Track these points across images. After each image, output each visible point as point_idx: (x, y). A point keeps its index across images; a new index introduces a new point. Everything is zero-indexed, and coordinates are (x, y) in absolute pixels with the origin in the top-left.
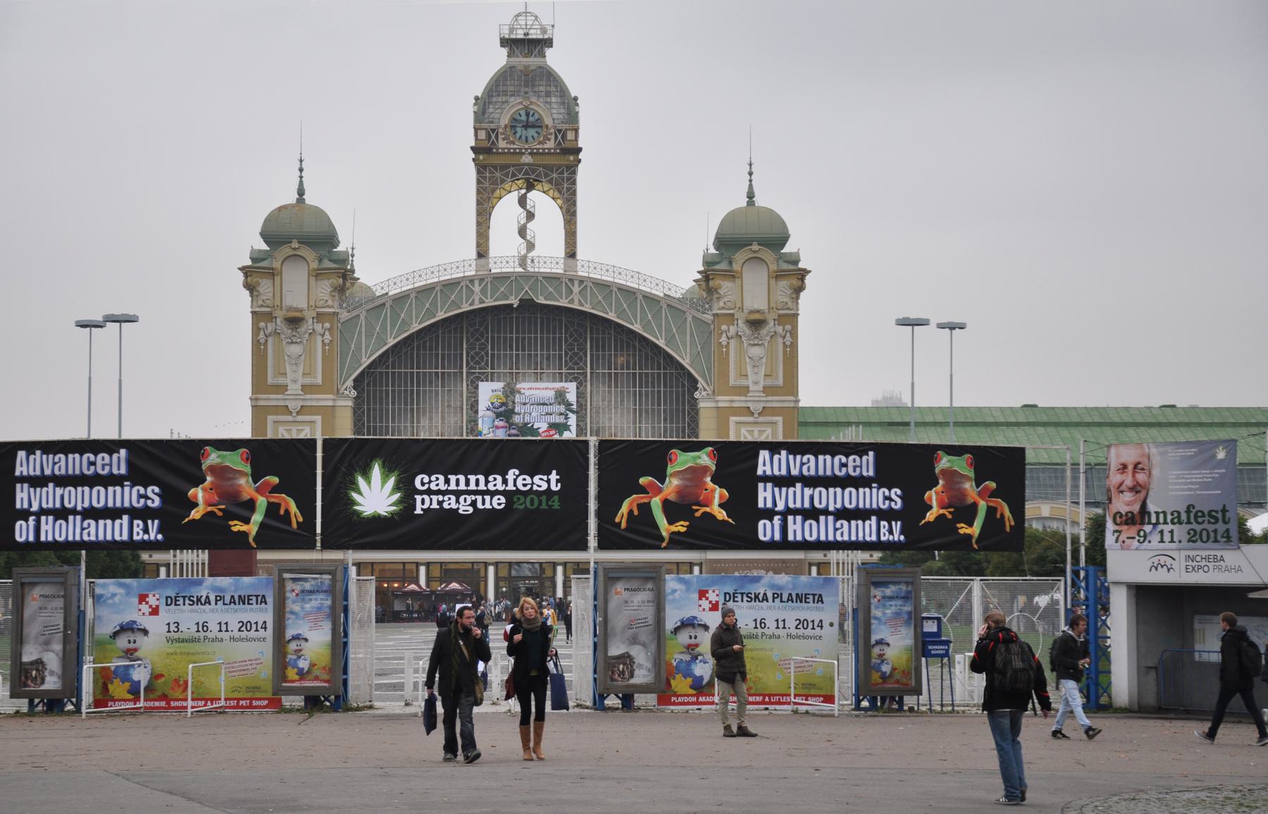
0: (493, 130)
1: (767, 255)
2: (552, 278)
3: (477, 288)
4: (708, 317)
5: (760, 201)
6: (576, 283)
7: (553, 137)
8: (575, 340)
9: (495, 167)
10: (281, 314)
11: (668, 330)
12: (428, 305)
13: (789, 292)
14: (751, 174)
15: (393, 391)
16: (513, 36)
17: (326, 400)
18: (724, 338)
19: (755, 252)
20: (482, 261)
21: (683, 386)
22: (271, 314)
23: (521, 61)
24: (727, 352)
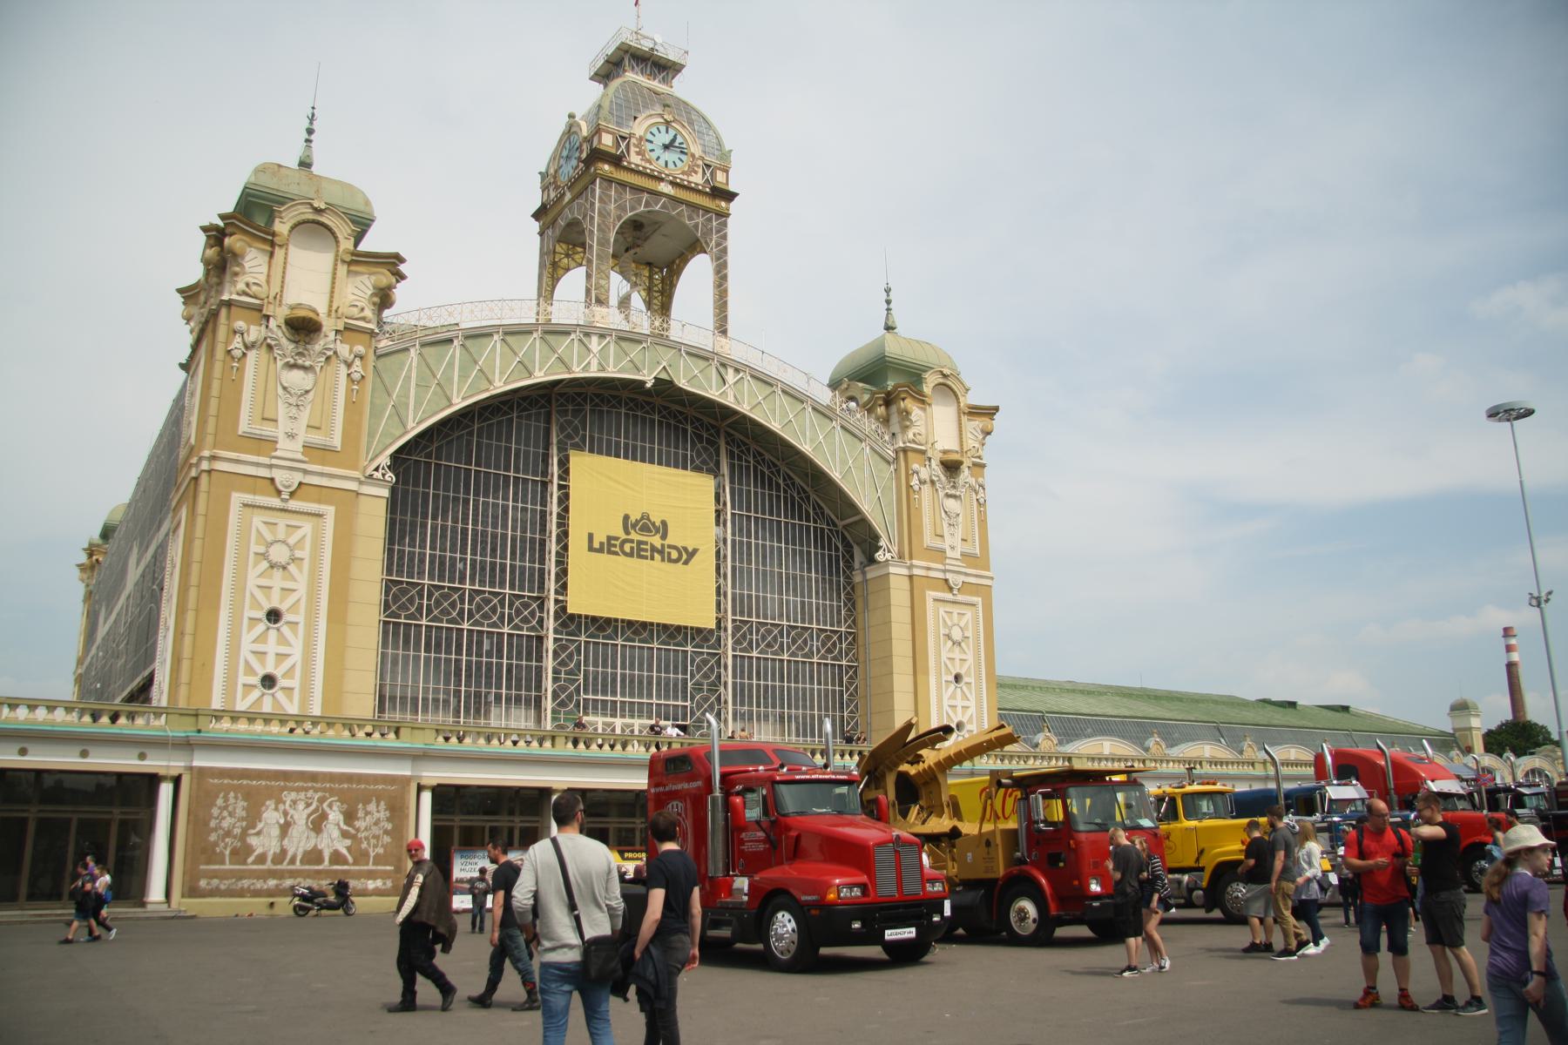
0: (624, 138)
10: (280, 314)
11: (844, 462)
15: (436, 496)
21: (837, 549)
22: (259, 309)
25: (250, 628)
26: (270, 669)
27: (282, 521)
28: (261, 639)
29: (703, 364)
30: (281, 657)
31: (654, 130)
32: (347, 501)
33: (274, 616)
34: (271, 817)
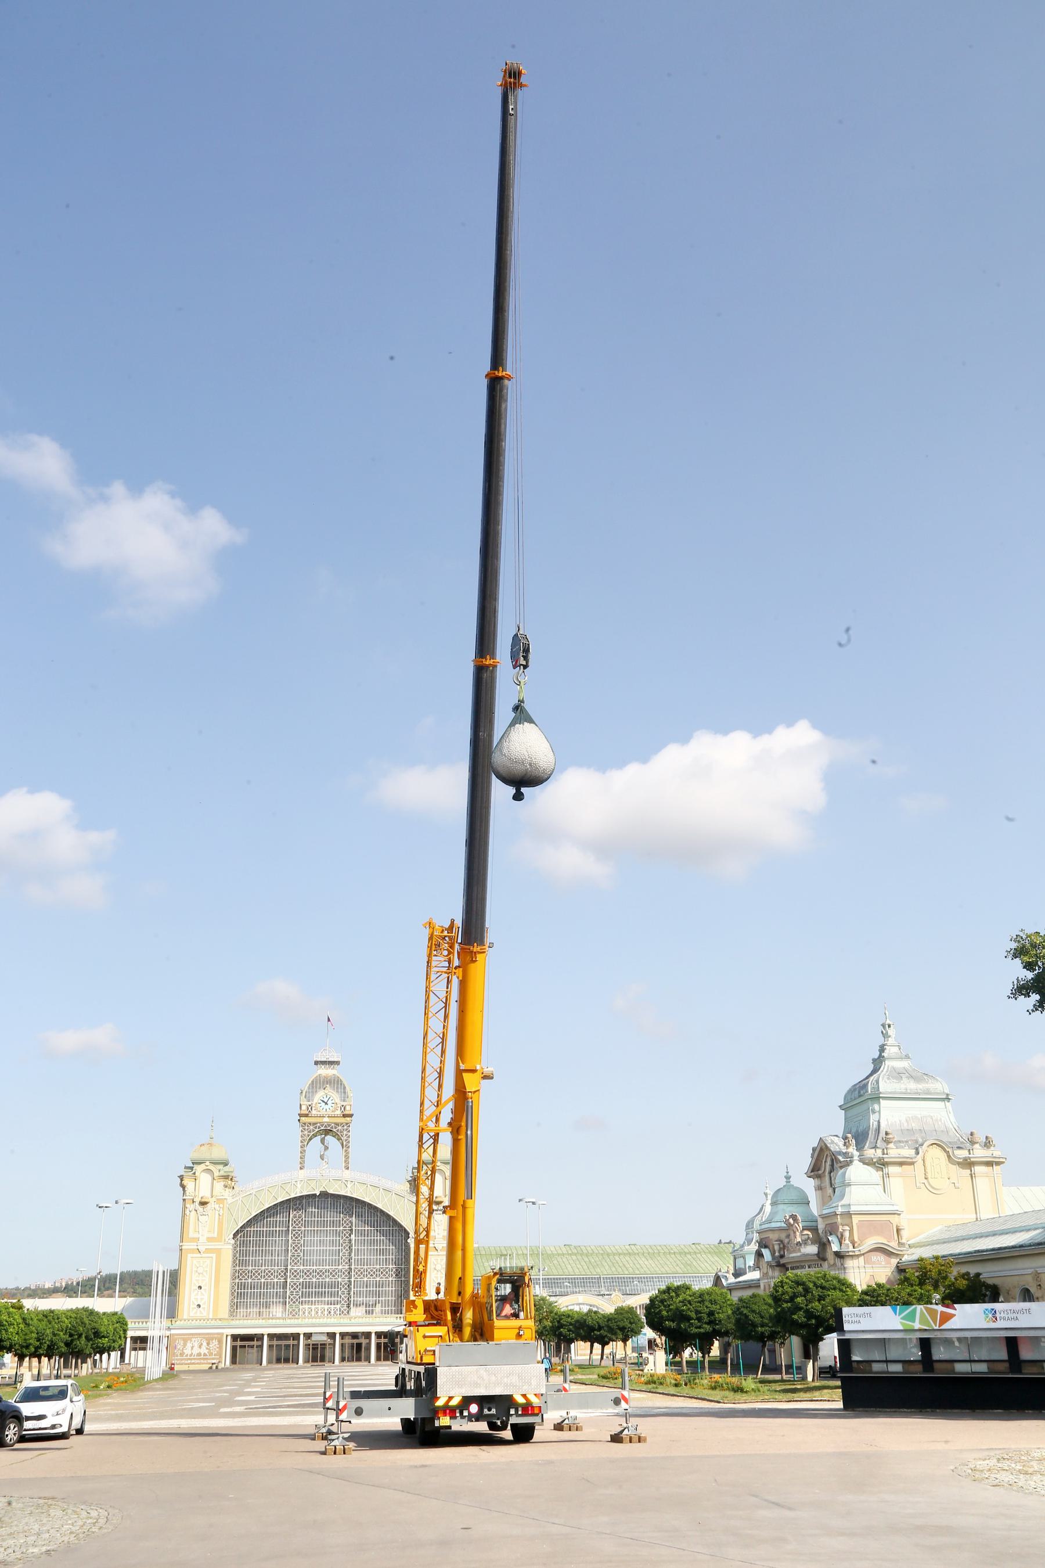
10: (197, 1200)
32: (218, 1252)
33: (200, 1287)
34: (189, 1345)
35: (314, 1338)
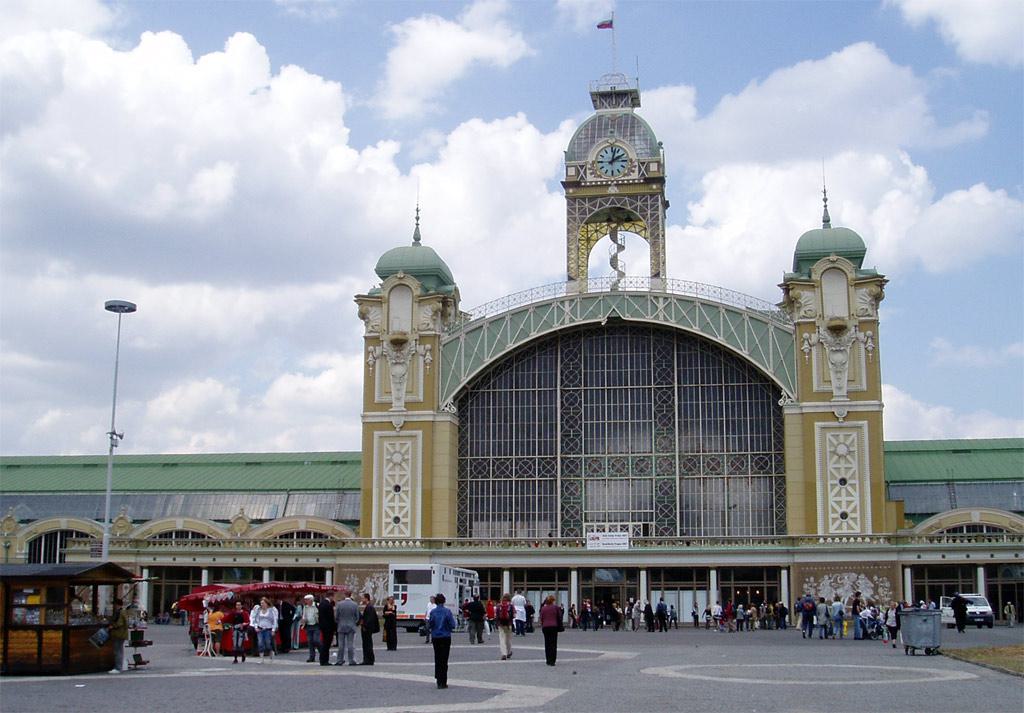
0: (582, 167)
1: (848, 266)
2: (638, 297)
3: (567, 308)
4: (790, 327)
5: (833, 224)
6: (661, 300)
7: (637, 169)
8: (664, 357)
9: (584, 199)
10: (386, 338)
12: (522, 326)
13: (869, 299)
14: (825, 200)
16: (602, 90)
17: (426, 415)
18: (806, 346)
19: (833, 262)
20: (572, 283)
21: (768, 397)
22: (377, 338)
23: (608, 111)
24: (810, 359)
25: (387, 495)
26: (397, 515)
27: (398, 443)
28: (392, 500)
29: (642, 300)
30: (401, 508)
31: (603, 153)
32: (430, 427)
33: (397, 488)
35: (605, 577)
